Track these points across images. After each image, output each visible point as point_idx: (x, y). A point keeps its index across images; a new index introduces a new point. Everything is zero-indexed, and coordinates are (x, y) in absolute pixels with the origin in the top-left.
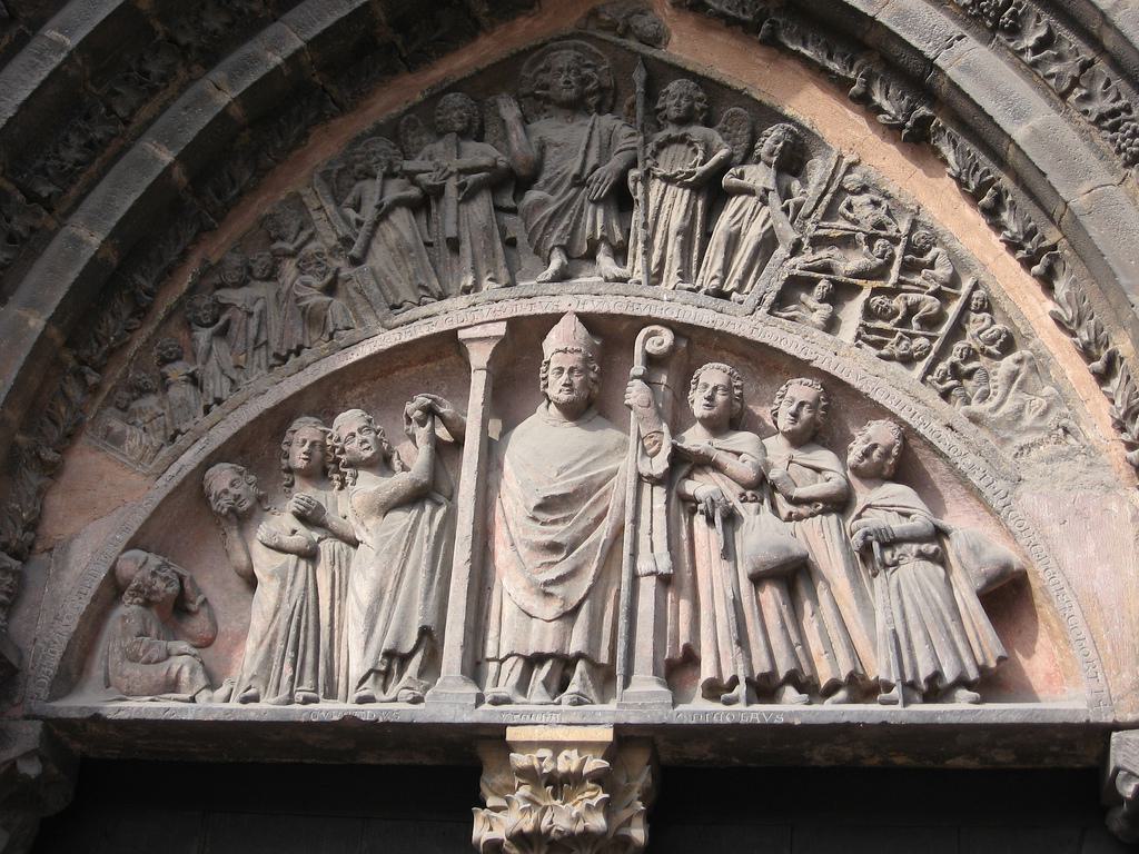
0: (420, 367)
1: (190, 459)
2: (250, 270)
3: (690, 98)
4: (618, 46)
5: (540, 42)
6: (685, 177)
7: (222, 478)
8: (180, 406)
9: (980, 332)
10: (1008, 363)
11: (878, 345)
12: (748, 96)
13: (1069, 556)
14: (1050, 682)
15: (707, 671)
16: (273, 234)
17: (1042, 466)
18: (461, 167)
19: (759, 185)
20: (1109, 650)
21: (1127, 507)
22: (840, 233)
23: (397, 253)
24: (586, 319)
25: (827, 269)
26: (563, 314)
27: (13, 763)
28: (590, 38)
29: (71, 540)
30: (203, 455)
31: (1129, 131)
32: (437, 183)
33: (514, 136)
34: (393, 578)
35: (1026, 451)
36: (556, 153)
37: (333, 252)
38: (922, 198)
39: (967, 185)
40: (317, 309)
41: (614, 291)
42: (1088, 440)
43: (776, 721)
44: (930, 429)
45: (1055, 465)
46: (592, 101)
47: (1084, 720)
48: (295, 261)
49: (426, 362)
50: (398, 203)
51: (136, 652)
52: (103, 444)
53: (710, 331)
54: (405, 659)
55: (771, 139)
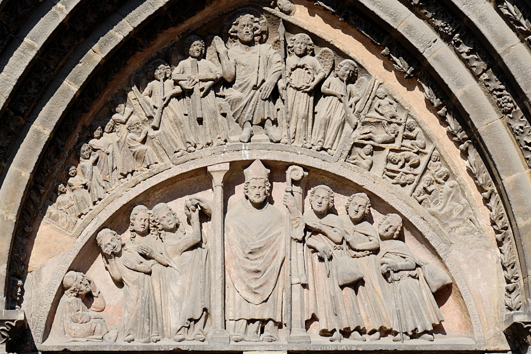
0: (188, 180)
3: (306, 44)
6: (305, 89)
8: (82, 201)
11: (392, 177)
19: (338, 92)
20: (485, 320)
21: (494, 257)
23: (174, 124)
24: (266, 163)
29: (41, 268)
30: (97, 226)
31: (506, 100)
32: (191, 88)
33: (224, 62)
34: (187, 285)
35: (454, 230)
36: (243, 69)
37: (144, 122)
40: (141, 153)
41: (277, 148)
42: (480, 225)
43: (352, 349)
44: (414, 219)
47: (474, 349)
49: (190, 178)
50: (172, 97)
51: (77, 318)
52: (49, 221)
54: (196, 321)
55: (344, 66)
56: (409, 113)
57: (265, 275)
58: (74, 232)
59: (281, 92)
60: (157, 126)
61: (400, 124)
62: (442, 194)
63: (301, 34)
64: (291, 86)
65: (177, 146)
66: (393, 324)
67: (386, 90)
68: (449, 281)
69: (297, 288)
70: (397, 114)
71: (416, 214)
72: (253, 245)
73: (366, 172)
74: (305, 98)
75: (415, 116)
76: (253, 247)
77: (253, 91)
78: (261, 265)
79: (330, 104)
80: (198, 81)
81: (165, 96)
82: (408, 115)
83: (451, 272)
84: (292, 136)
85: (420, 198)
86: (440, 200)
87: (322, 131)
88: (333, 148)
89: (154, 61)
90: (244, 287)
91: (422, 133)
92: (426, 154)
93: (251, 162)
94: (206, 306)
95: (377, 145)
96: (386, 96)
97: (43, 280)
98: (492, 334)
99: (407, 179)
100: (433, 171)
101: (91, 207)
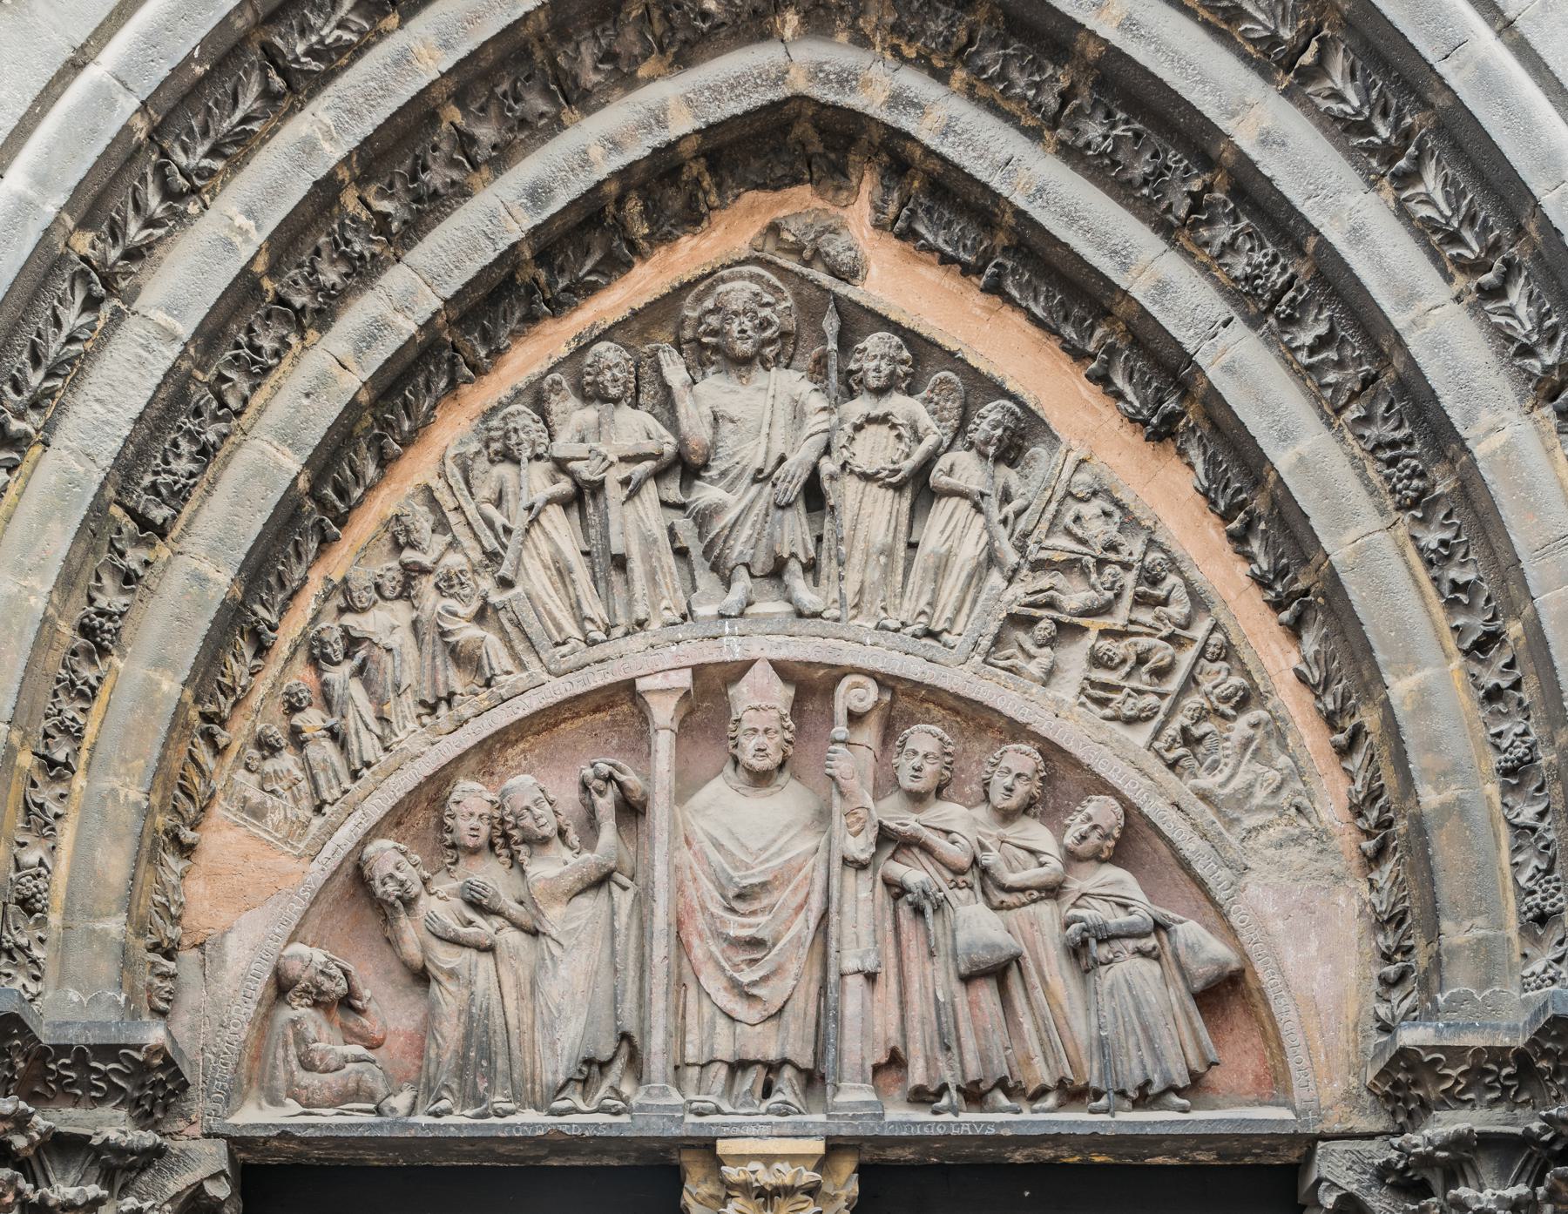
1: (346, 837)
2: (378, 587)
3: (892, 360)
4: (803, 279)
5: (708, 270)
7: (386, 856)
9: (1215, 687)
10: (1241, 726)
11: (1102, 703)
12: (962, 360)
13: (1290, 957)
14: (1259, 1085)
15: (917, 1075)
16: (402, 539)
17: (1270, 852)
18: (622, 454)
21: (1355, 901)
22: (1065, 556)
24: (782, 670)
25: (1051, 604)
26: (754, 662)
27: (199, 1187)
28: (768, 264)
29: (224, 935)
32: (597, 478)
38: (1161, 511)
39: (1214, 503)
40: (470, 648)
41: (812, 630)
45: (1284, 851)
46: (769, 351)
48: (432, 579)
50: (549, 502)
53: (918, 685)
54: (604, 1066)
55: (990, 418)
56: (1154, 537)
57: (775, 951)
58: (302, 846)
59: (826, 485)
60: (510, 576)
61: (1127, 567)
62: (1228, 744)
63: (880, 334)
64: (852, 472)
65: (560, 629)
66: (1092, 1075)
67: (1096, 477)
68: (1235, 965)
69: (855, 983)
70: (1120, 538)
71: (1161, 795)
72: (745, 877)
73: (1036, 689)
74: (888, 502)
75: (1167, 545)
76: (745, 883)
77: (756, 488)
78: (766, 926)
79: (951, 517)
80: (615, 459)
81: (532, 500)
82: (1151, 543)
83: (1243, 939)
84: (851, 599)
85: (1171, 756)
86: (1223, 760)
87: (929, 587)
88: (957, 630)
89: (506, 411)
90: (723, 982)
91: (1183, 589)
92: (1193, 641)
93: (749, 665)
94: (627, 1028)
95: (1065, 618)
96: (1095, 494)
97: (229, 964)
98: (1338, 1094)
99: (1141, 705)
100: (1207, 687)
101: (347, 784)
